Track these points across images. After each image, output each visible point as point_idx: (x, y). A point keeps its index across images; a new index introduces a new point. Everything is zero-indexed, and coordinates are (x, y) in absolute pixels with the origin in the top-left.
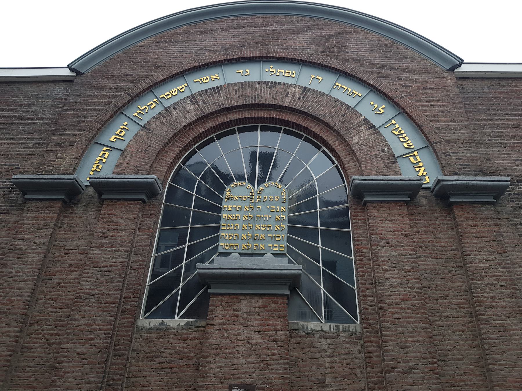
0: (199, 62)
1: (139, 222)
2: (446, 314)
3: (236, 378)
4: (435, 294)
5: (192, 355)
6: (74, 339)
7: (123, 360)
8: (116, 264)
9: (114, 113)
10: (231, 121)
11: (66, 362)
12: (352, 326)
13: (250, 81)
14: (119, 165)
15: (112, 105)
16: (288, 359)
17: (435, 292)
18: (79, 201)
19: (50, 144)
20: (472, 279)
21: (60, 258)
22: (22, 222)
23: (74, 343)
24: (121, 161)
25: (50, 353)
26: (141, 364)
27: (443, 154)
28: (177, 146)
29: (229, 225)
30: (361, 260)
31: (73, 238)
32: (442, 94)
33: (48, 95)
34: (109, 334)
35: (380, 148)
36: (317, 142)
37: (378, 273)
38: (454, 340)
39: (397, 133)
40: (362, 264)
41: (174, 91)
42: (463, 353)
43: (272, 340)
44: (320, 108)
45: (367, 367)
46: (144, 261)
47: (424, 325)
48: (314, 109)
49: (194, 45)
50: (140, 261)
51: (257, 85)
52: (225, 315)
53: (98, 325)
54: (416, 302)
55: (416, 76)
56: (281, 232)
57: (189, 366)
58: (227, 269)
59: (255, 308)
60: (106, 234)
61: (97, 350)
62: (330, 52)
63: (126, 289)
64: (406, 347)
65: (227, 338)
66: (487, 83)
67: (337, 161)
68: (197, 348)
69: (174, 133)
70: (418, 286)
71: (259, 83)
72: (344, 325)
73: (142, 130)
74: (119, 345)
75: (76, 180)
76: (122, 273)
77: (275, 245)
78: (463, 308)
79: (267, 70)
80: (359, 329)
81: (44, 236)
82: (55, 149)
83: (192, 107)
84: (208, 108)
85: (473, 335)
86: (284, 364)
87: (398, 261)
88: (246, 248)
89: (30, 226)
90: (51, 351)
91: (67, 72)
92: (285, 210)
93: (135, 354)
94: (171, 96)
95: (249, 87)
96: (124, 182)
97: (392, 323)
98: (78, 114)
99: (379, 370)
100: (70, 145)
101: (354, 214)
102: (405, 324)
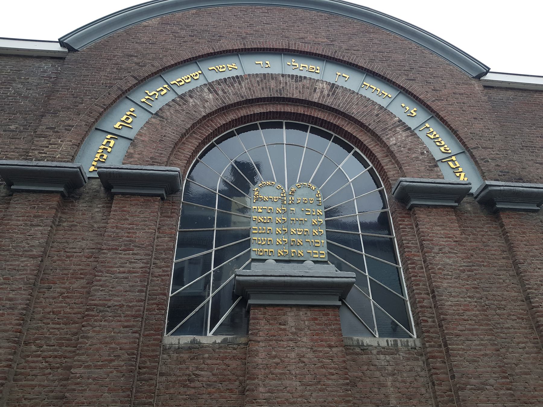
0: (213, 49)
1: (158, 221)
2: (507, 325)
3: (291, 403)
4: (494, 304)
5: (234, 377)
6: (87, 362)
7: (150, 386)
8: (135, 270)
9: (118, 97)
10: (254, 114)
11: (79, 390)
12: (409, 339)
13: (273, 73)
14: (129, 156)
15: (115, 88)
16: (347, 379)
17: (492, 302)
18: (80, 195)
19: (40, 127)
20: (529, 288)
21: (60, 262)
22: (8, 217)
23: (88, 367)
24: (132, 151)
25: (54, 381)
26: (172, 391)
27: (482, 159)
28: (196, 138)
29: (260, 228)
30: (414, 268)
31: (76, 239)
32: (472, 101)
33: (32, 71)
34: (133, 354)
35: (420, 150)
36: (346, 141)
37: (435, 281)
38: (518, 353)
39: (432, 137)
40: (415, 272)
41: (186, 77)
42: (530, 366)
43: (327, 358)
44: (351, 106)
45: (433, 384)
46: (167, 267)
47: (490, 337)
48: (346, 107)
49: (206, 31)
50: (163, 267)
51: (281, 78)
52: (270, 330)
53: (118, 344)
54: (478, 312)
55: (445, 81)
56: (320, 238)
57: (231, 391)
58: (271, 276)
59: (304, 321)
60: (120, 235)
61: (119, 374)
62: (354, 50)
63: (149, 300)
64: (475, 361)
65: (275, 357)
66: (510, 93)
67: (372, 163)
68: (238, 369)
69: (192, 123)
70: (478, 295)
71: (283, 75)
72: (402, 339)
73: (154, 118)
74: (144, 368)
75: (80, 170)
76: (144, 281)
77: (314, 251)
78: (522, 319)
79: (289, 64)
80: (418, 344)
81: (39, 236)
82: (47, 133)
83: (211, 96)
84: (229, 98)
85: (537, 347)
86: (343, 385)
87: (454, 269)
88: (282, 254)
89: (19, 223)
90: (55, 378)
91: (57, 47)
92: (321, 213)
93: (164, 378)
94: (183, 83)
95: (272, 79)
96: (141, 174)
97: (458, 335)
98: (73, 95)
99: (448, 388)
100: (66, 130)
101: (400, 219)
102: (471, 337)
